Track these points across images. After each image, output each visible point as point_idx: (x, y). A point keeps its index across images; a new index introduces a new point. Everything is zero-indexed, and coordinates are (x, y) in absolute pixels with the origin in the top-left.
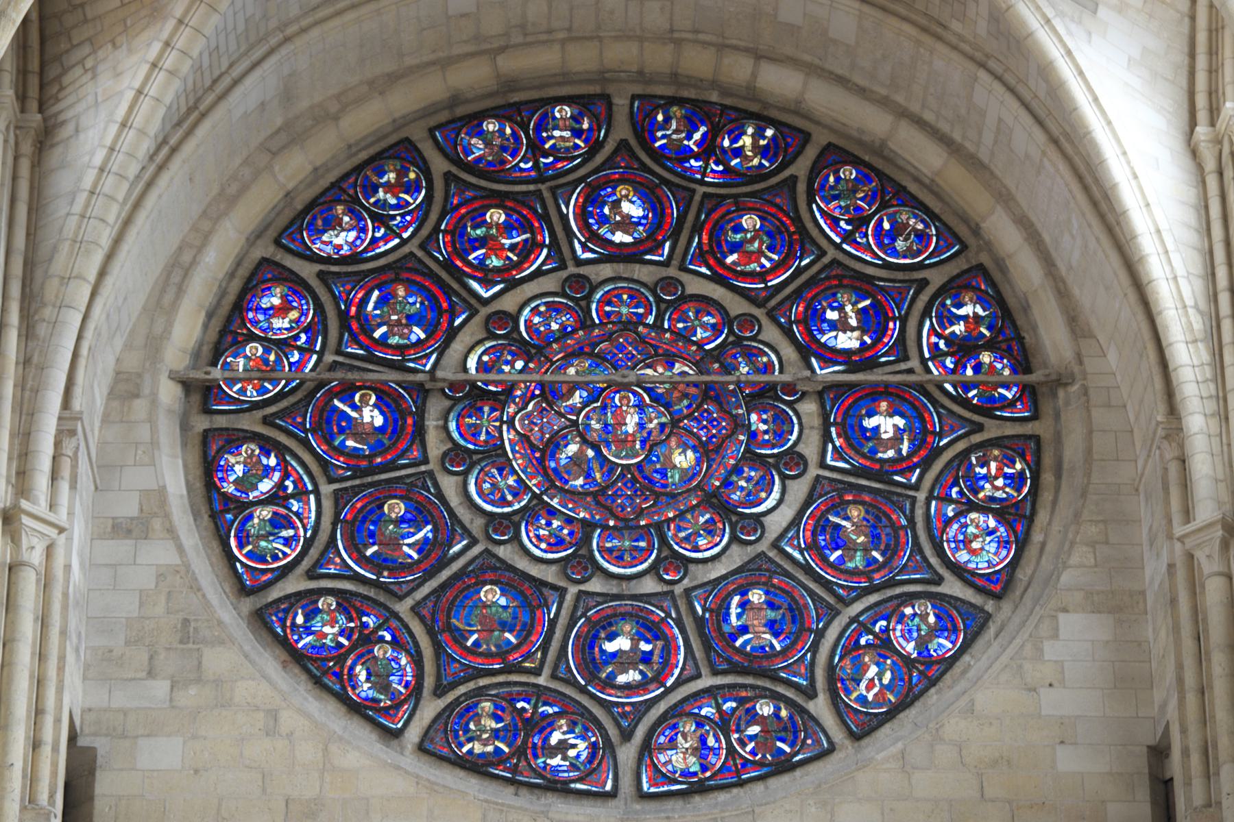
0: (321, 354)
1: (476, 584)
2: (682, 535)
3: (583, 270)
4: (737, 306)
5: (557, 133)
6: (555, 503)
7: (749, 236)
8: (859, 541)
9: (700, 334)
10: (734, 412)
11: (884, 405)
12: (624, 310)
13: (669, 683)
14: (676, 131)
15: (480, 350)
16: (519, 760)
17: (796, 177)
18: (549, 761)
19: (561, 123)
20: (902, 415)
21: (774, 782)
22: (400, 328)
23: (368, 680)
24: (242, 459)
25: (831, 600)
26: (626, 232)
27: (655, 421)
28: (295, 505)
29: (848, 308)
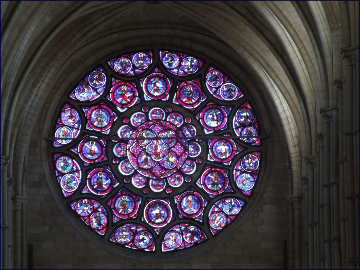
0: (81, 130)
1: (121, 195)
2: (172, 181)
3: (147, 104)
4: (187, 114)
5: (140, 62)
6: (140, 172)
7: (189, 93)
8: (215, 182)
9: (176, 123)
10: (185, 145)
11: (223, 144)
12: (157, 116)
13: (169, 222)
14: (171, 61)
15: (121, 128)
16: (132, 244)
17: (201, 74)
18: (140, 243)
19: (141, 59)
20: (228, 145)
21: (194, 248)
22: (101, 122)
23: (96, 222)
24: (62, 161)
25: (208, 199)
26: (158, 92)
27: (165, 149)
28: (76, 174)
29: (214, 114)
